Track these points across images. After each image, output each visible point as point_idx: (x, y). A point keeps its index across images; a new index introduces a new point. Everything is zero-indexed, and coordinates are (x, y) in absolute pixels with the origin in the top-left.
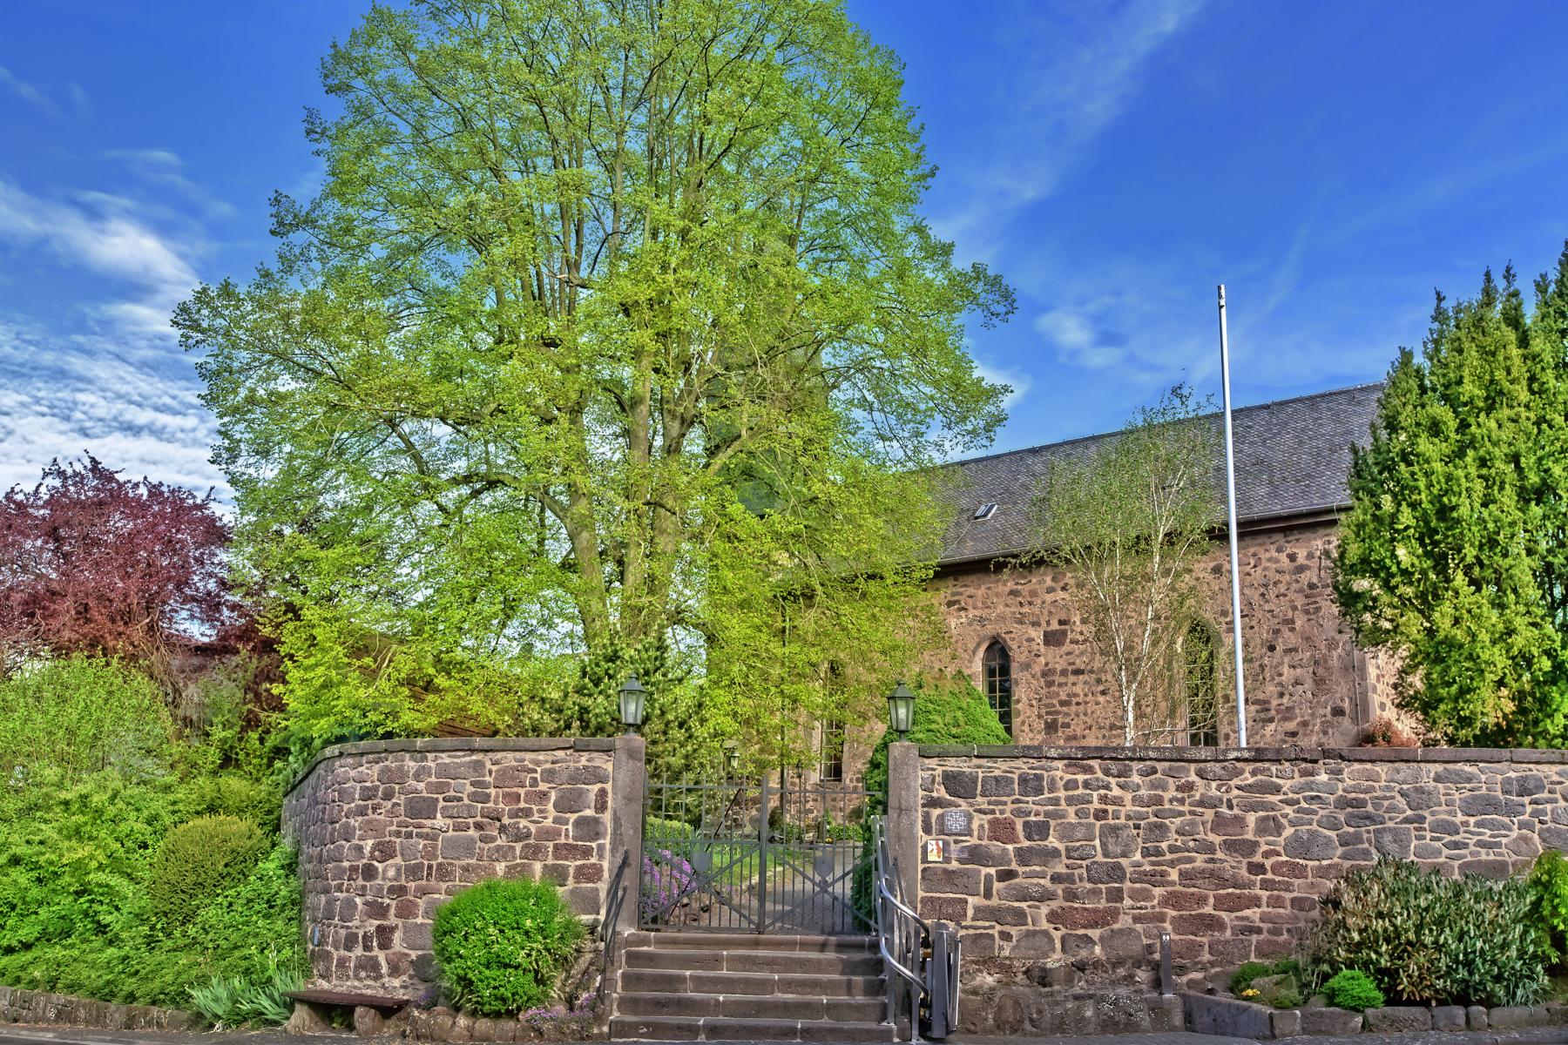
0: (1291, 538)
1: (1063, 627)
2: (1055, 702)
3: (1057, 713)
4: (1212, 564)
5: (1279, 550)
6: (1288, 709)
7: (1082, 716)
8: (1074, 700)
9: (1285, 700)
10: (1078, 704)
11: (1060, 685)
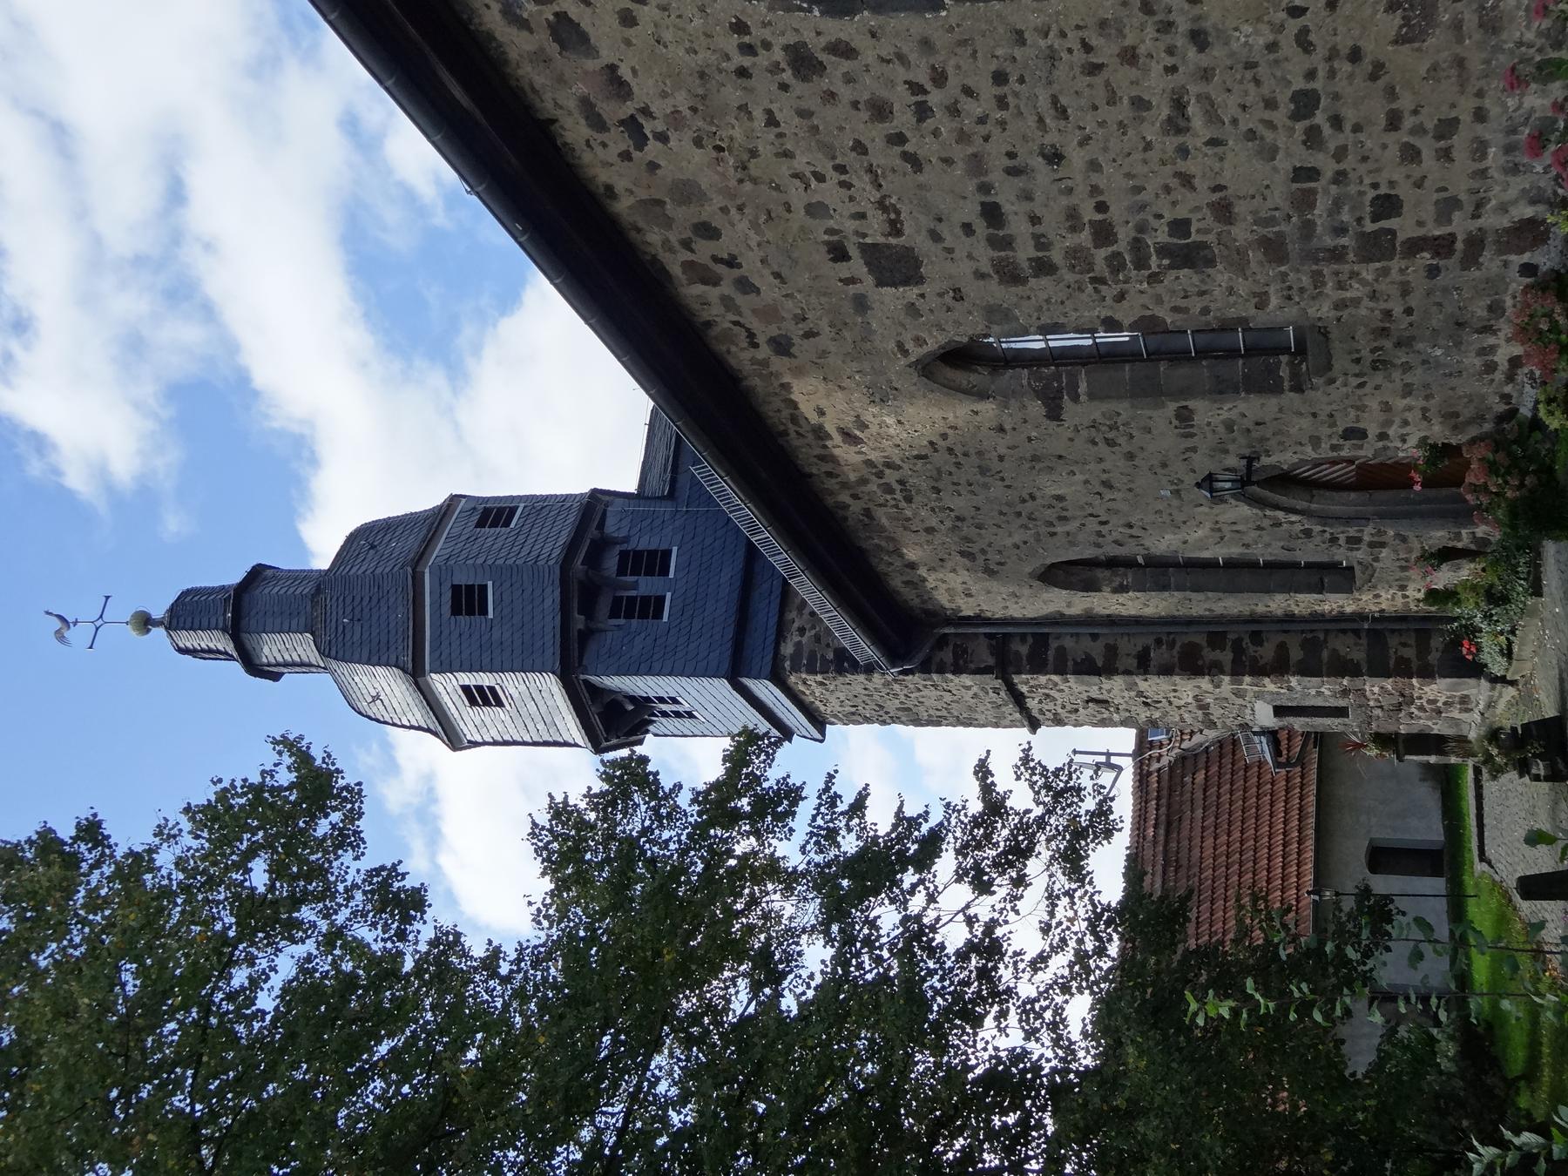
1: (853, 251)
2: (1102, 254)
3: (1137, 245)
7: (1143, 197)
8: (1088, 214)
10: (1101, 207)
11: (1041, 243)
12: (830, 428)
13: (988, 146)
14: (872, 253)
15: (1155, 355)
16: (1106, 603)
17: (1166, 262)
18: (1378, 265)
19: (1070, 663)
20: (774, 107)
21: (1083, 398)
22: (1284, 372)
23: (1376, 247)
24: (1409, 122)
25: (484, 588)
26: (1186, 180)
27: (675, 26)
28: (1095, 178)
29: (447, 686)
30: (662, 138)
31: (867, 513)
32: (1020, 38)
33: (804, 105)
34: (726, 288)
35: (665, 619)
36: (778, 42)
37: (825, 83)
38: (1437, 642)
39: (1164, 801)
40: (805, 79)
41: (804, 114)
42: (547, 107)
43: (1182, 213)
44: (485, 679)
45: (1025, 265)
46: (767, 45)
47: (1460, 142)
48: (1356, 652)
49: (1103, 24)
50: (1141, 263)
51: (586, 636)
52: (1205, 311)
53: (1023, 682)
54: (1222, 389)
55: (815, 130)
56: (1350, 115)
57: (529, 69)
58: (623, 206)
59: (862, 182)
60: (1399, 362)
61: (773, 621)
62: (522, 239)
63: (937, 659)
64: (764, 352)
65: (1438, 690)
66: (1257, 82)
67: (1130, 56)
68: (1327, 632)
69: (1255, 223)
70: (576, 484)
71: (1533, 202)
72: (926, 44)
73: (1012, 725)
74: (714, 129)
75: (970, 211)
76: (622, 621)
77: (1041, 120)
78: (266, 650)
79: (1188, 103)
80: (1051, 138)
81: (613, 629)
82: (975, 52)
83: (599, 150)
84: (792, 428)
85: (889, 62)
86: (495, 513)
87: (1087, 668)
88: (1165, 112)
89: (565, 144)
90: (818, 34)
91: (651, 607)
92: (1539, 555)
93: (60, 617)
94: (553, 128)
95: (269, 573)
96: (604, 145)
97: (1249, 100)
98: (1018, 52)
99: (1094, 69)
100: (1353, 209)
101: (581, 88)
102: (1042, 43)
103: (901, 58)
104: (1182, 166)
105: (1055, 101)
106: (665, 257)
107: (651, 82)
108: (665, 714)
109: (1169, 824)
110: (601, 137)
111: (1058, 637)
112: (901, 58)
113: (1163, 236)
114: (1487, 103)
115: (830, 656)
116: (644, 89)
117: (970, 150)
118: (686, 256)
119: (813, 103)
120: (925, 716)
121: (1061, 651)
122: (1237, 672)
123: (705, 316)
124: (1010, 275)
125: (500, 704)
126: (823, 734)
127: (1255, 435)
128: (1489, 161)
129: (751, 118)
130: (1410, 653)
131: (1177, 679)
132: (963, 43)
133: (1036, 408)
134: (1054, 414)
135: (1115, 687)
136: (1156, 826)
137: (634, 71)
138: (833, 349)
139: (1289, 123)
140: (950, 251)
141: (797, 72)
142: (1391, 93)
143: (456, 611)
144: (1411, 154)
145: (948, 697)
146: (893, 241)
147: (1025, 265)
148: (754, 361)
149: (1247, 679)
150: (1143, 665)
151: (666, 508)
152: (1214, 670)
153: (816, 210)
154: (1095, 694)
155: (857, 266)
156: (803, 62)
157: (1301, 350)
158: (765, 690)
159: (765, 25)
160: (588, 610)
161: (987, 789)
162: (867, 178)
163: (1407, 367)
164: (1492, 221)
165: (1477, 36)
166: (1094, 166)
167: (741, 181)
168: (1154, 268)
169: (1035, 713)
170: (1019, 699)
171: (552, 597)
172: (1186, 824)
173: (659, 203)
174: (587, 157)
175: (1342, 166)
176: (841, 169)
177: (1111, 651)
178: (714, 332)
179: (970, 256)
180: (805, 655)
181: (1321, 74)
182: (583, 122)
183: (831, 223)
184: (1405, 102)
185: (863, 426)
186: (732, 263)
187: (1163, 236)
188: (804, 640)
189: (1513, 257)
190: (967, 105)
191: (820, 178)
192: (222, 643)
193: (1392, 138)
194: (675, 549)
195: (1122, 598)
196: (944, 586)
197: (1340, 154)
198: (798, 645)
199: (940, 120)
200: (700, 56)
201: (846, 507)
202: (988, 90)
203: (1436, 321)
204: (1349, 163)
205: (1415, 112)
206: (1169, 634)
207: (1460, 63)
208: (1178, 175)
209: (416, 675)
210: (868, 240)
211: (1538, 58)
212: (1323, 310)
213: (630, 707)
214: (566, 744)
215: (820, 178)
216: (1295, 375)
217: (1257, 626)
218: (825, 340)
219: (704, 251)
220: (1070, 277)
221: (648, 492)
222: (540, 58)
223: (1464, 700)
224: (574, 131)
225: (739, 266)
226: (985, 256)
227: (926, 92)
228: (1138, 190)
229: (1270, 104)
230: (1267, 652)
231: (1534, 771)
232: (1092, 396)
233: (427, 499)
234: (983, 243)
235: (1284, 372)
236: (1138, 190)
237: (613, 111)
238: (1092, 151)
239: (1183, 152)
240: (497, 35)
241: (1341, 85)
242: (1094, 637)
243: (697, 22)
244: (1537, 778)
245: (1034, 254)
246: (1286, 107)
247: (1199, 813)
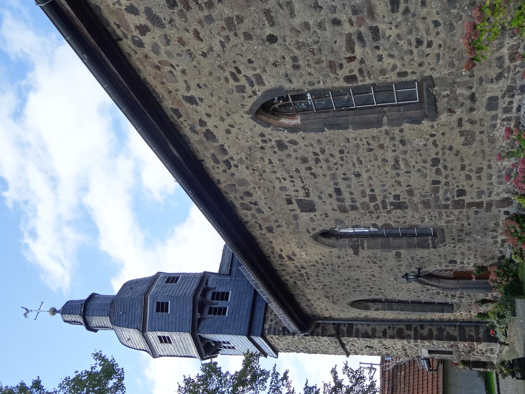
0: (119, 32)
1: (294, 201)
2: (372, 204)
3: (383, 202)
4: (187, 105)
5: (140, 44)
6: (355, 11)
7: (385, 188)
8: (368, 192)
9: (344, 18)
10: (372, 190)
11: (353, 200)
12: (284, 255)
13: (337, 171)
14: (300, 202)
15: (388, 235)
16: (372, 314)
17: (392, 207)
18: (459, 210)
19: (360, 334)
20: (271, 158)
21: (366, 248)
22: (430, 242)
23: (458, 204)
24: (468, 168)
25: (167, 303)
26: (399, 183)
27: (242, 134)
28: (370, 182)
29: (153, 336)
30: (236, 166)
31: (295, 283)
32: (348, 141)
33: (280, 158)
34: (253, 211)
35: (227, 315)
36: (274, 140)
37: (287, 152)
38: (482, 330)
39: (391, 381)
40: (282, 150)
41: (281, 160)
42: (201, 156)
43: (397, 193)
44: (166, 334)
45: (348, 207)
46: (270, 140)
47: (484, 174)
48: (455, 333)
49: (373, 137)
50: (385, 207)
51: (200, 320)
52: (405, 222)
53: (344, 340)
54: (410, 246)
55: (284, 165)
56: (449, 166)
57: (197, 145)
58: (222, 186)
59: (298, 181)
60: (466, 240)
61: (262, 316)
62: (191, 196)
63: (316, 331)
64: (264, 231)
65: (482, 346)
66: (421, 155)
67: (381, 147)
68: (445, 325)
69: (420, 196)
70: (199, 270)
71: (507, 193)
72: (319, 142)
73: (341, 354)
74: (253, 164)
75: (331, 190)
76: (212, 316)
77: (354, 164)
78: (94, 322)
79: (399, 160)
80: (357, 170)
81: (210, 319)
82: (334, 144)
83: (216, 169)
84: (272, 255)
85: (307, 146)
86: (172, 279)
87: (366, 335)
88: (393, 163)
89: (206, 167)
90: (286, 137)
91: (222, 311)
92: (514, 303)
93: (26, 309)
94: (202, 162)
95: (96, 296)
96: (218, 168)
97: (419, 160)
98: (347, 145)
99: (370, 150)
100: (451, 193)
101: (212, 151)
102: (355, 142)
103: (312, 145)
104: (397, 179)
105: (358, 159)
106: (234, 201)
107: (234, 150)
108: (225, 347)
109: (393, 389)
110: (217, 165)
111: (356, 325)
112: (312, 145)
113: (391, 199)
114: (492, 163)
115: (281, 329)
116: (232, 152)
117: (332, 172)
118: (241, 201)
119: (284, 157)
120: (311, 350)
121: (357, 330)
122: (416, 339)
123: (246, 219)
124: (343, 210)
125: (170, 342)
126: (278, 356)
127: (421, 261)
128: (493, 180)
129: (264, 161)
130: (473, 333)
131: (396, 340)
132: (331, 141)
133: (351, 251)
134: (356, 253)
135: (375, 342)
136: (388, 390)
137: (229, 147)
138: (286, 231)
139: (431, 167)
140: (324, 202)
141: (279, 148)
142: (462, 159)
143: (158, 311)
144: (469, 177)
145: (319, 344)
146: (306, 198)
147: (348, 207)
148: (261, 234)
149: (419, 341)
150: (384, 335)
151: (228, 278)
152: (408, 337)
153: (283, 189)
154: (368, 344)
155: (295, 206)
156: (281, 145)
157: (435, 235)
158: (259, 340)
159: (270, 134)
160: (201, 311)
161: (335, 378)
162: (299, 180)
163: (469, 242)
164: (494, 198)
165: (488, 144)
166: (370, 178)
167: (260, 180)
168: (389, 209)
169: (348, 350)
170: (343, 345)
171: (190, 307)
172: (398, 389)
173: (234, 185)
174: (212, 171)
175: (447, 180)
176: (291, 177)
177: (374, 330)
178: (249, 225)
179: (331, 204)
180: (273, 328)
181: (440, 153)
182: (212, 161)
183: (287, 193)
184: (467, 162)
185: (295, 255)
186: (256, 204)
187: (391, 199)
188: (272, 323)
189: (502, 209)
190: (332, 159)
191: (285, 179)
192: (80, 319)
193: (462, 173)
194: (230, 292)
195: (377, 312)
196: (319, 307)
197: (447, 177)
198: (270, 325)
199: (323, 164)
200: (250, 143)
201: (288, 280)
202: (338, 155)
203: (478, 228)
204: (450, 179)
205: (470, 165)
206: (393, 325)
207: (483, 152)
208: (396, 181)
209: (143, 332)
210: (299, 198)
211: (507, 151)
212: (442, 223)
213: (214, 345)
214: (192, 357)
215: (285, 179)
216: (433, 243)
217: (422, 323)
218: (283, 229)
219: (247, 200)
220: (362, 211)
221: (222, 273)
222: (201, 142)
223: (492, 350)
224: (209, 164)
225: (258, 205)
226: (335, 204)
227: (318, 155)
228: (384, 185)
229: (425, 162)
230: (425, 332)
231: (517, 376)
232: (368, 248)
233: (150, 273)
234: (335, 200)
235: (430, 242)
236: (384, 185)
237: (222, 158)
238: (370, 174)
239: (398, 175)
240: (188, 135)
241: (446, 157)
242: (368, 325)
243: (249, 133)
244: (518, 378)
245: (351, 204)
246: (430, 163)
247: (403, 386)
